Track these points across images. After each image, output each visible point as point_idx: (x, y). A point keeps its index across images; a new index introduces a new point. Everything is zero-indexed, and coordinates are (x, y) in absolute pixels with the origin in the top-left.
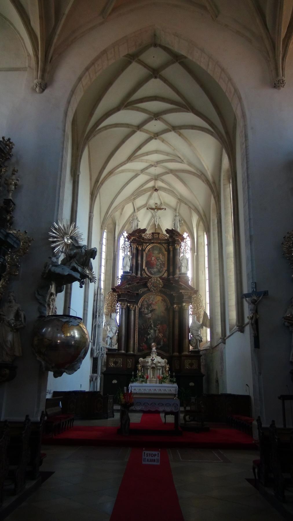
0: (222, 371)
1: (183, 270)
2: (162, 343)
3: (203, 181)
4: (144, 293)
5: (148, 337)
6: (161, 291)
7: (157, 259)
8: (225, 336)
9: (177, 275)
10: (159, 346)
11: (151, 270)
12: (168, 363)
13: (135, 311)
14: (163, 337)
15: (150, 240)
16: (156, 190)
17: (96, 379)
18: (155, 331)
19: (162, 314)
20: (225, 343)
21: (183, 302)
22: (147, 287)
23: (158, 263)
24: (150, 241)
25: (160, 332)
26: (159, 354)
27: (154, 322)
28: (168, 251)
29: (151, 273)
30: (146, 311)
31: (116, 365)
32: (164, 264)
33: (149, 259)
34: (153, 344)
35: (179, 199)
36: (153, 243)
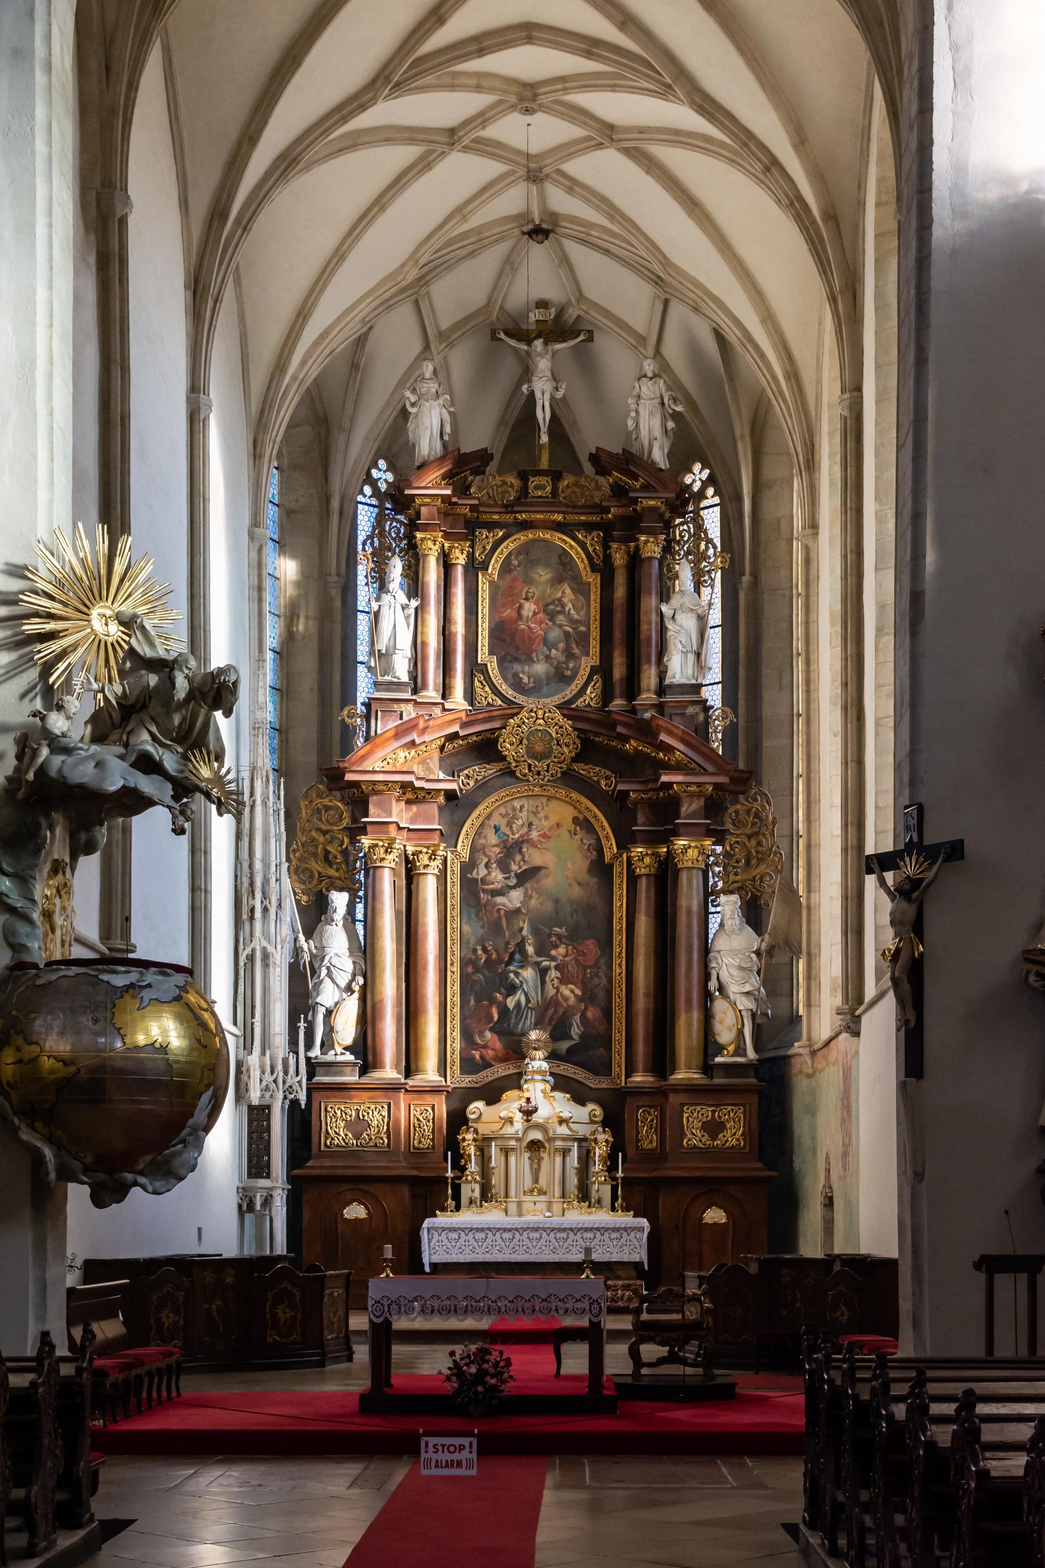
0: (845, 1155)
1: (679, 668)
2: (575, 1031)
3: (779, 202)
4: (484, 789)
5: (511, 1003)
6: (569, 779)
7: (551, 610)
8: (860, 999)
9: (647, 697)
10: (564, 1046)
11: (517, 667)
12: (605, 1123)
13: (442, 878)
14: (580, 999)
15: (509, 508)
16: (539, 233)
17: (267, 1201)
18: (543, 972)
19: (576, 892)
20: (857, 1034)
21: (676, 833)
22: (503, 758)
23: (555, 634)
24: (509, 518)
25: (563, 981)
26: (561, 1084)
27: (535, 931)
28: (605, 569)
29: (517, 685)
30: (497, 876)
31: (357, 1137)
32: (583, 640)
33: (508, 613)
34: (534, 1035)
35: (658, 281)
36: (525, 526)
